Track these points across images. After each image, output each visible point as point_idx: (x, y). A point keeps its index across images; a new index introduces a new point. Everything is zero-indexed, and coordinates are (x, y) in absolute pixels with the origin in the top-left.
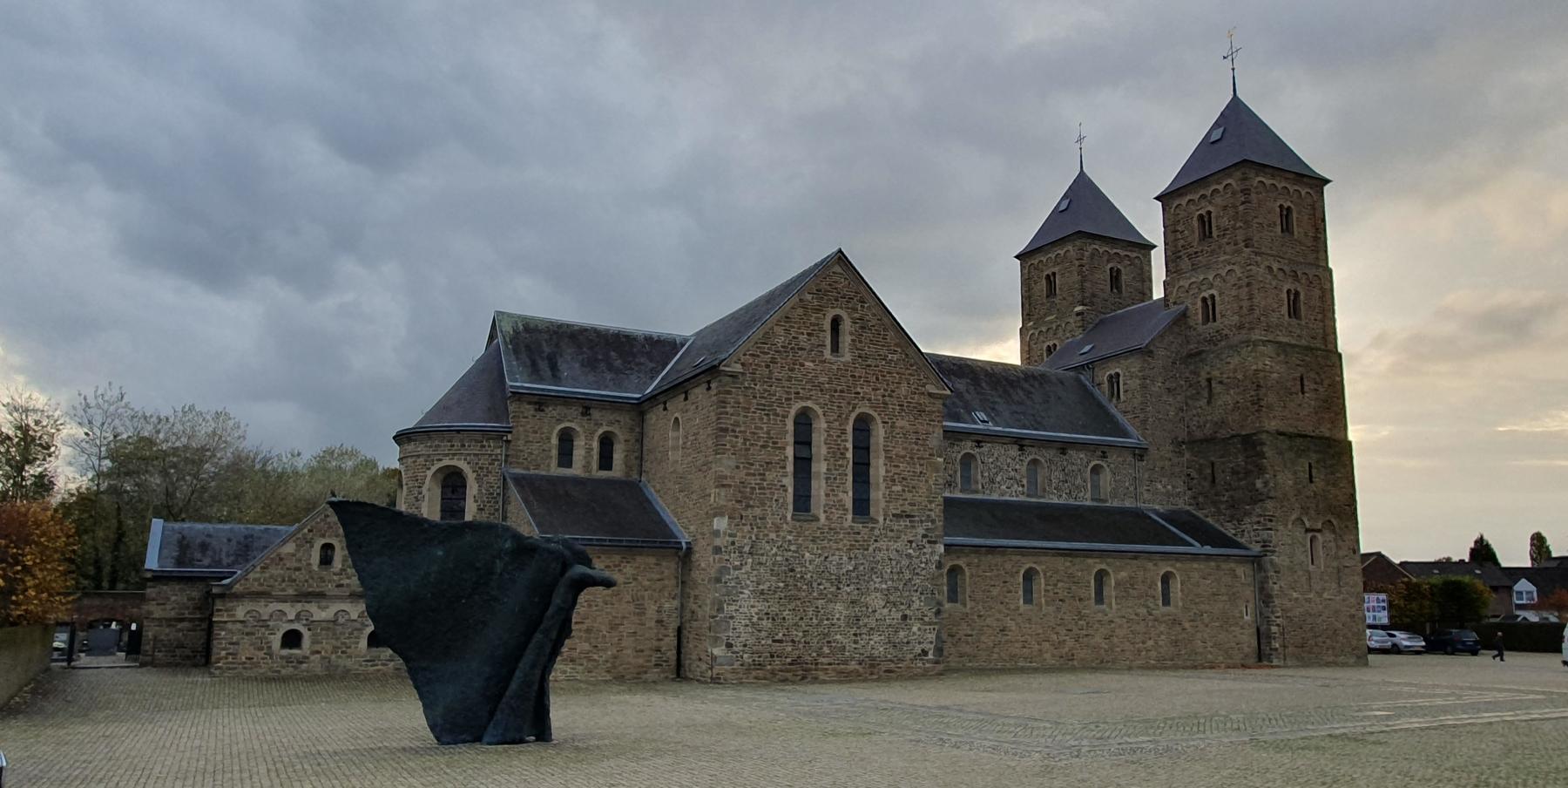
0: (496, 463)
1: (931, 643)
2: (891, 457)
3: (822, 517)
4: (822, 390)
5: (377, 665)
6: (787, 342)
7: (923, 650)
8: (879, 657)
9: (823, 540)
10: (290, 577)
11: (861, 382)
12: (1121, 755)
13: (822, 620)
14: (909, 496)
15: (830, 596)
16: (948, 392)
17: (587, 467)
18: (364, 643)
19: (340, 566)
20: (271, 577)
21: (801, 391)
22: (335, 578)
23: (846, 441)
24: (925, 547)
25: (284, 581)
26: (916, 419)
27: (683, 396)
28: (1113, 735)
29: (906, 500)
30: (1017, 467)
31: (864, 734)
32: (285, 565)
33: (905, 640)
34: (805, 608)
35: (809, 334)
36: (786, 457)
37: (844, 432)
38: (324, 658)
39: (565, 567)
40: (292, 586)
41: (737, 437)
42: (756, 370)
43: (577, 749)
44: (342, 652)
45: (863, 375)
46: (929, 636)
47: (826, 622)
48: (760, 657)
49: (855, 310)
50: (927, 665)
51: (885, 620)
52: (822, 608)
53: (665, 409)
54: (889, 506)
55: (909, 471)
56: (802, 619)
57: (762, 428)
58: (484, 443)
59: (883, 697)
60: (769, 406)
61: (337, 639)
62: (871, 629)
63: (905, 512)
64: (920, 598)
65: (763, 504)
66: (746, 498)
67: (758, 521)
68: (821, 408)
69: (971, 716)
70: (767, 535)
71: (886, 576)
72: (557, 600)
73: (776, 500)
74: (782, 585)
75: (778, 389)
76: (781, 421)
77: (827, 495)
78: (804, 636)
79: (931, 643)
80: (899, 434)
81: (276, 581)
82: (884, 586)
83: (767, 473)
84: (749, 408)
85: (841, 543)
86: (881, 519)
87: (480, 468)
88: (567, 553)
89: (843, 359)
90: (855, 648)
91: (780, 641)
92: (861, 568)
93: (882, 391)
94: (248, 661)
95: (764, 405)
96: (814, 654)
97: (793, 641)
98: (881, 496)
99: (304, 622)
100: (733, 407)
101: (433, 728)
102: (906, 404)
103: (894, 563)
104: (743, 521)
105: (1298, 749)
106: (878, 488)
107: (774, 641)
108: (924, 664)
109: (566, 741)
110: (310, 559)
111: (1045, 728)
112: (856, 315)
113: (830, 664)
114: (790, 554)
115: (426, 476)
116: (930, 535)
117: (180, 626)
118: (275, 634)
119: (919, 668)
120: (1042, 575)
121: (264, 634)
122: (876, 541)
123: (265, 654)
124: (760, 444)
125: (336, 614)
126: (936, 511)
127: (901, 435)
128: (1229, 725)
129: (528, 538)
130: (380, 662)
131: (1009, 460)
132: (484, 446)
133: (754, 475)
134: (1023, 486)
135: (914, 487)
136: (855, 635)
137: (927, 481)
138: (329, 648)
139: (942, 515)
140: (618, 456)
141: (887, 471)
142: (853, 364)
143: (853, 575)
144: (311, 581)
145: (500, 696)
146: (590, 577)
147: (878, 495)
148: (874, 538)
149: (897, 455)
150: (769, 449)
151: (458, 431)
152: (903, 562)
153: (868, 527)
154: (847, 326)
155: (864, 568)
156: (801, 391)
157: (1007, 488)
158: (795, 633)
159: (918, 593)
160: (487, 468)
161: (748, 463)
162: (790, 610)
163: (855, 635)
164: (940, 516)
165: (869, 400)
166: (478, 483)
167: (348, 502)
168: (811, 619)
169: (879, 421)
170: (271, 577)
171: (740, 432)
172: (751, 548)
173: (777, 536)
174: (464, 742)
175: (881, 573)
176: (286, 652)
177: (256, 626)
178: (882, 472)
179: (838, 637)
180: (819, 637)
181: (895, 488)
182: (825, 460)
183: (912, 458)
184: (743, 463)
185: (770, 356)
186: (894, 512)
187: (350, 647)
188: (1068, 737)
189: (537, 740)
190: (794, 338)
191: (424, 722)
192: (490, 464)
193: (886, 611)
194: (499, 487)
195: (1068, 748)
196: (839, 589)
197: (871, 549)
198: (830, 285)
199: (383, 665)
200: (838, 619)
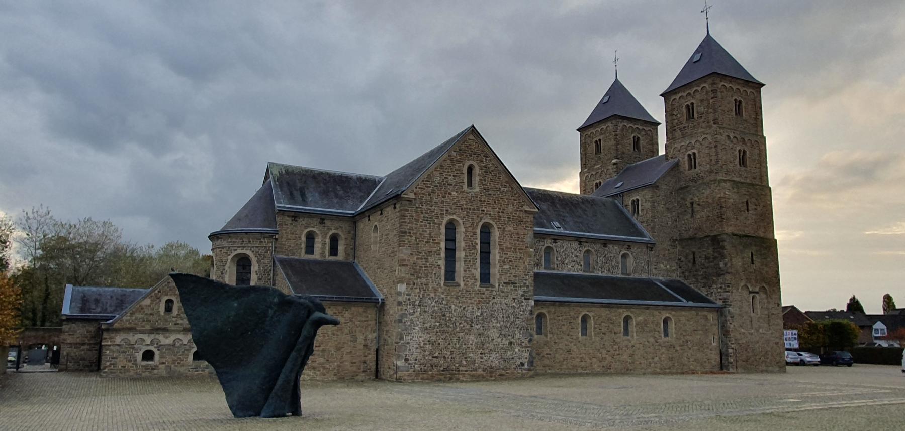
1: (526, 358)
2: (503, 249)
3: (462, 284)
4: (462, 209)
6: (441, 180)
7: (521, 363)
9: (462, 298)
11: (485, 204)
12: (639, 425)
13: (462, 345)
14: (513, 271)
15: (466, 331)
16: (537, 210)
17: (323, 254)
18: (191, 358)
19: (177, 313)
20: (136, 319)
21: (449, 209)
22: (174, 319)
23: (477, 239)
24: (522, 302)
25: (144, 321)
26: (517, 226)
27: (380, 212)
28: (634, 413)
29: (512, 274)
30: (578, 254)
31: (486, 412)
33: (511, 357)
34: (452, 338)
35: (454, 176)
36: (441, 249)
37: (475, 234)
39: (310, 312)
40: (148, 324)
41: (411, 236)
42: (423, 197)
43: (317, 420)
45: (486, 200)
46: (526, 354)
47: (464, 346)
48: (425, 367)
49: (482, 161)
50: (524, 372)
51: (499, 345)
52: (462, 338)
53: (369, 220)
54: (501, 278)
55: (513, 257)
57: (426, 231)
59: (498, 391)
60: (430, 218)
61: (175, 355)
62: (491, 350)
63: (511, 281)
64: (519, 332)
65: (427, 276)
66: (417, 273)
67: (424, 286)
68: (461, 219)
69: (550, 402)
70: (429, 295)
71: (499, 319)
72: (304, 332)
74: (438, 324)
75: (436, 208)
76: (437, 227)
77: (465, 271)
78: (451, 354)
79: (526, 358)
80: (507, 235)
82: (498, 325)
83: (429, 258)
84: (419, 220)
85: (473, 299)
86: (497, 285)
88: (311, 305)
89: (474, 191)
90: (481, 362)
91: (437, 357)
92: (485, 314)
93: (498, 209)
94: (123, 369)
95: (428, 218)
96: (457, 365)
97: (444, 357)
98: (497, 272)
99: (156, 345)
100: (409, 219)
101: (231, 408)
102: (512, 217)
103: (504, 311)
104: (415, 287)
105: (744, 421)
106: (495, 267)
107: (433, 357)
108: (522, 371)
109: (310, 415)
110: (159, 309)
111: (594, 409)
112: (482, 164)
113: (466, 371)
114: (443, 305)
115: (227, 259)
116: (525, 294)
117: (82, 347)
118: (138, 352)
119: (519, 373)
120: (592, 318)
122: (494, 298)
124: (425, 240)
125: (174, 341)
126: (530, 281)
127: (509, 236)
128: (703, 407)
129: (288, 296)
130: (200, 369)
131: (573, 251)
132: (262, 242)
133: (422, 259)
134: (581, 266)
135: (516, 267)
136: (481, 354)
137: (524, 263)
139: (533, 283)
140: (341, 248)
141: (500, 257)
142: (481, 193)
143: (480, 318)
144: (159, 321)
145: (271, 389)
146: (324, 318)
147: (495, 271)
148: (492, 296)
149: (506, 248)
150: (431, 243)
151: (247, 233)
152: (510, 311)
153: (489, 290)
154: (477, 170)
155: (487, 314)
156: (449, 209)
157: (572, 267)
158: (446, 352)
159: (519, 329)
160: (264, 255)
161: (418, 252)
162: (442, 339)
163: (481, 354)
164: (532, 284)
165: (490, 215)
167: (181, 274)
168: (455, 344)
169: (495, 227)
170: (136, 319)
171: (414, 233)
172: (420, 302)
173: (436, 295)
174: (250, 416)
175: (497, 317)
176: (145, 363)
178: (497, 257)
179: (471, 355)
181: (505, 267)
182: (464, 250)
183: (515, 249)
184: (415, 252)
185: (431, 188)
186: (505, 281)
187: (182, 361)
188: (607, 414)
189: (293, 415)
190: (445, 178)
191: (226, 405)
192: (265, 252)
193: (499, 340)
194: (271, 266)
195: (608, 421)
197: (490, 303)
198: (467, 146)
199: (202, 371)
200: (471, 344)
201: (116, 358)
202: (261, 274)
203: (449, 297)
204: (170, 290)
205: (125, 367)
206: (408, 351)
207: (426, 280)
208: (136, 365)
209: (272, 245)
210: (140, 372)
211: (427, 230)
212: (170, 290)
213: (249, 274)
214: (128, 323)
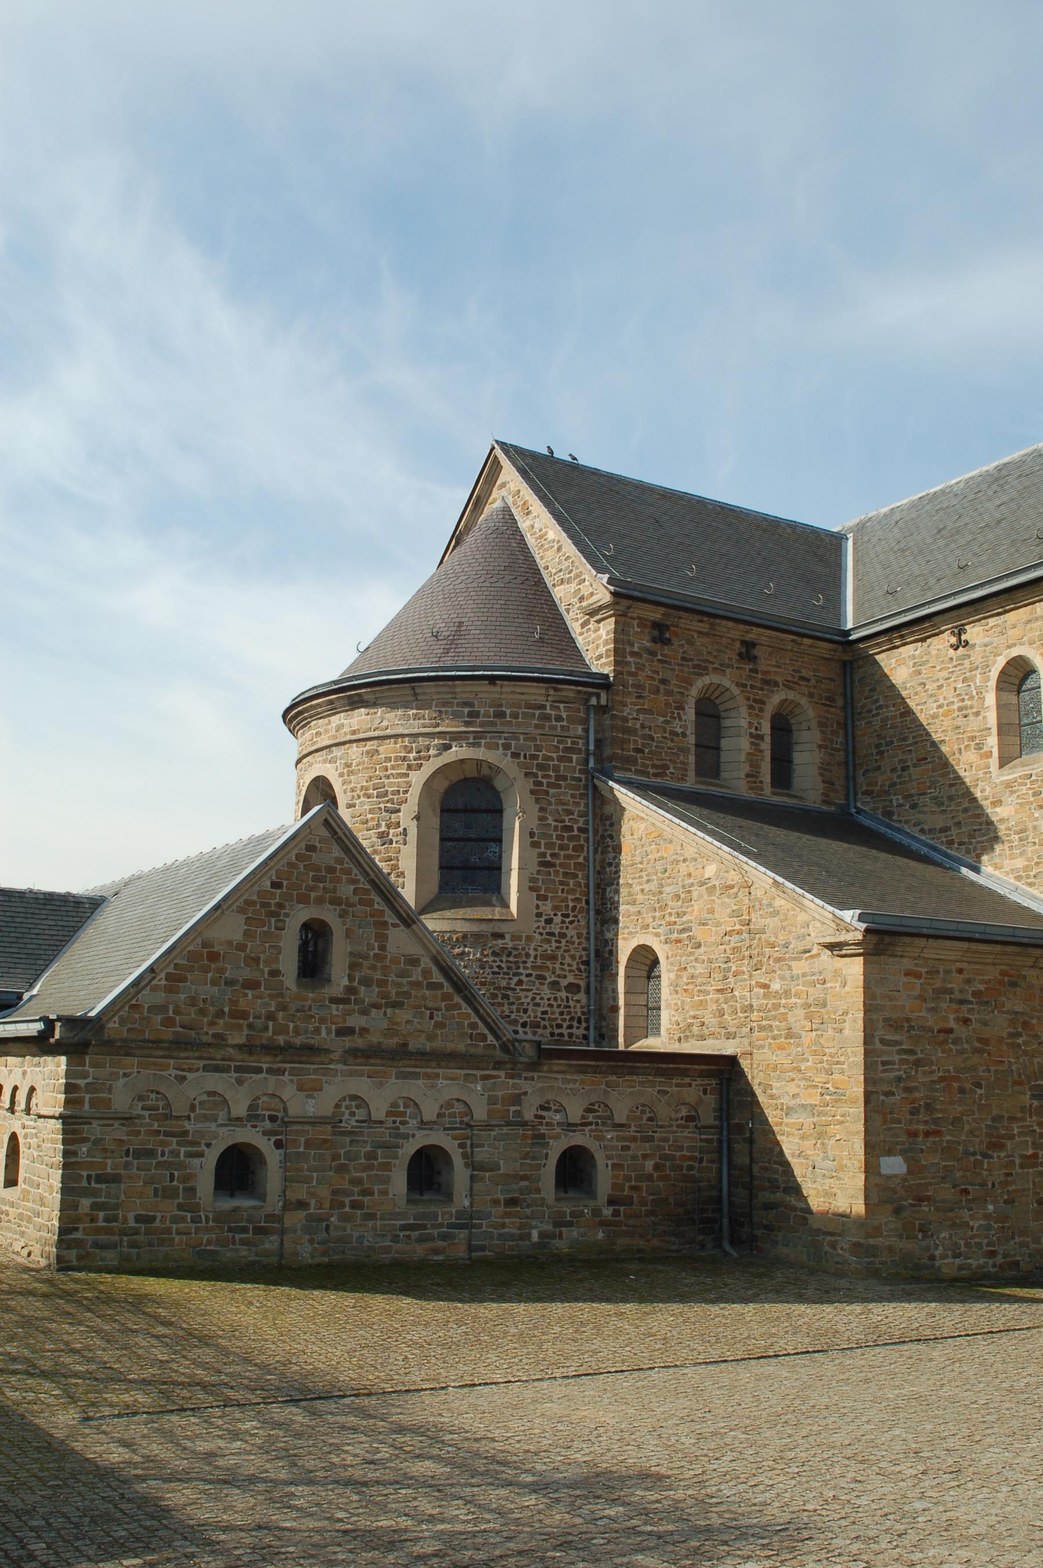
0: (574, 757)
5: (430, 1238)
10: (234, 1002)
17: (753, 776)
18: (399, 1182)
19: (345, 982)
20: (193, 1001)
22: (335, 1010)
25: (220, 1014)
32: (222, 970)
38: (310, 1218)
40: (239, 1027)
44: (354, 1205)
58: (548, 711)
61: (342, 1169)
81: (202, 1012)
87: (540, 767)
99: (267, 1125)
110: (277, 960)
118: (201, 1155)
121: (178, 1155)
123: (180, 1207)
125: (337, 1106)
130: (436, 1232)
132: (546, 718)
138: (324, 1192)
151: (492, 680)
160: (556, 769)
166: (537, 801)
170: (193, 1001)
176: (227, 1204)
177: (159, 1132)
187: (371, 1193)
192: (560, 759)
194: (585, 814)
199: (444, 1237)
201: (115, 1179)
202: (550, 845)
204: (317, 879)
205: (153, 1219)
208: (194, 1208)
209: (587, 731)
210: (209, 1242)
212: (317, 879)
213: (494, 847)
214: (159, 1018)
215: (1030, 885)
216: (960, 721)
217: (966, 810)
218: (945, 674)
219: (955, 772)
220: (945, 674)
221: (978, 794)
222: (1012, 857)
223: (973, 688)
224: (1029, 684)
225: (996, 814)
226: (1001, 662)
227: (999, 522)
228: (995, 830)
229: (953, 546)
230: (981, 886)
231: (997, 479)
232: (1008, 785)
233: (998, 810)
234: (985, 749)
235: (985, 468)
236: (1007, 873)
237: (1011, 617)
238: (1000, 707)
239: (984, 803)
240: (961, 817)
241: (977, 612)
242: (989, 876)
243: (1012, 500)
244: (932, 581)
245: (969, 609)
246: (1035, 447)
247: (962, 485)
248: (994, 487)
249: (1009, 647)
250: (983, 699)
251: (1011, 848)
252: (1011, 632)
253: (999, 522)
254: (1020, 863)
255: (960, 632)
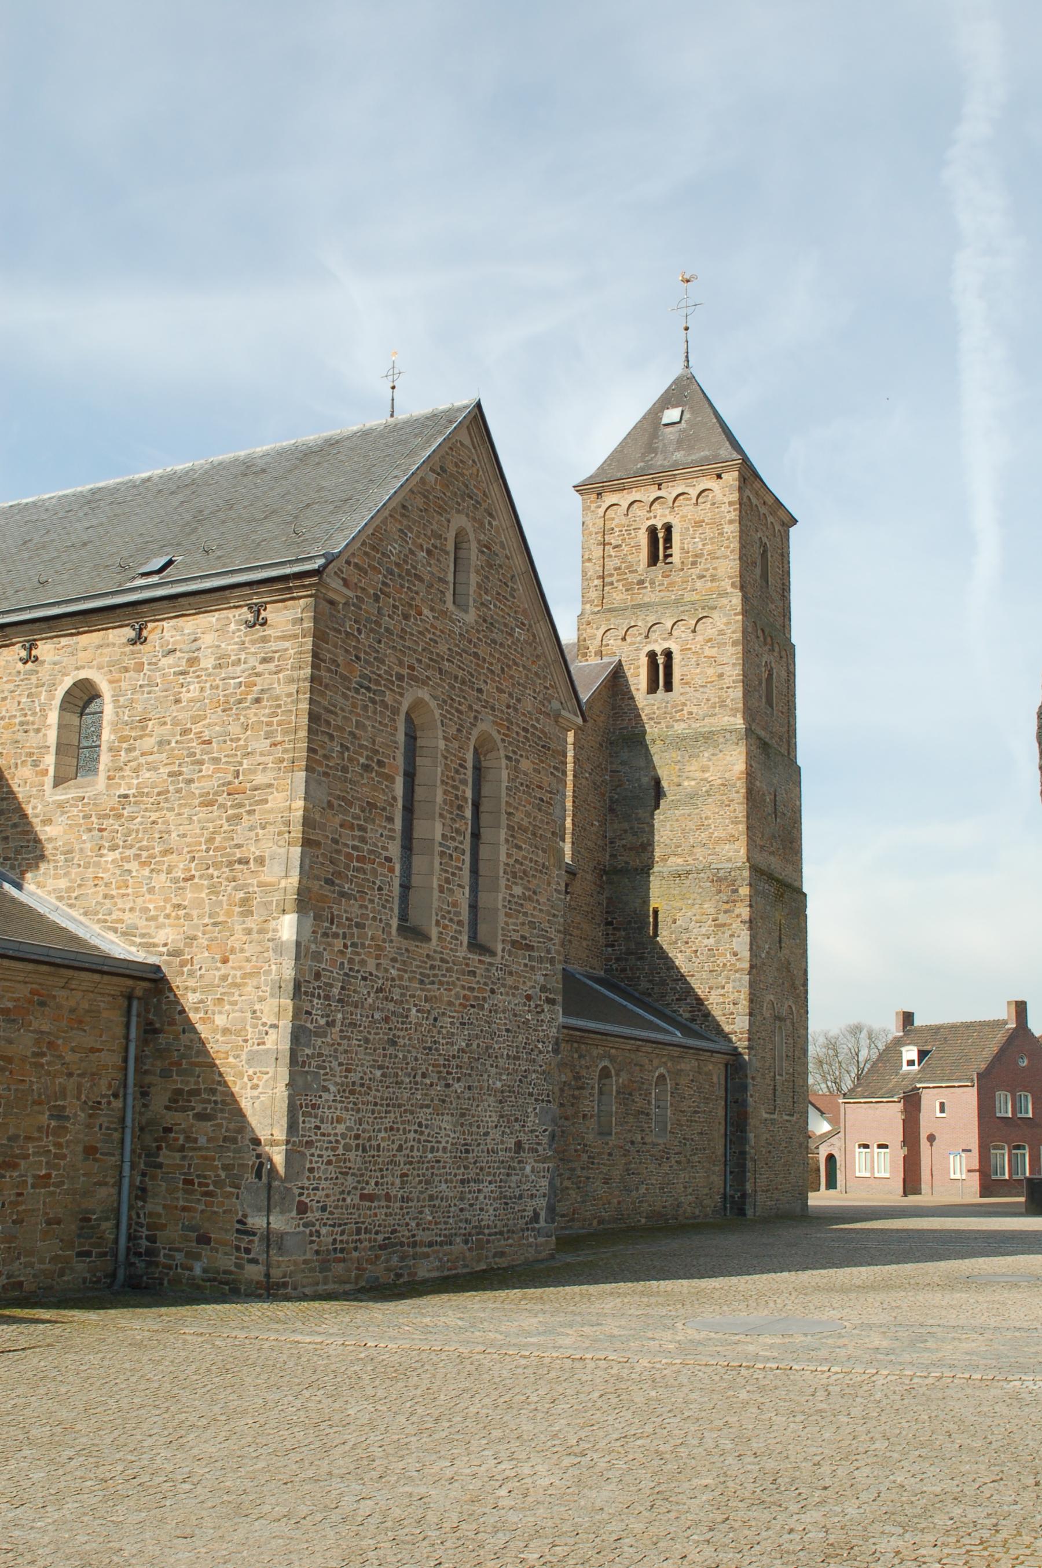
8: (488, 1227)
27: (129, 633)
36: (394, 798)
56: (400, 1148)
70: (363, 962)
73: (380, 889)
74: (378, 1073)
83: (369, 827)
97: (388, 1197)
106: (495, 889)
107: (363, 1197)
150: (374, 774)
172: (343, 988)
180: (419, 1188)
196: (448, 1086)
203: (406, 976)
206: (307, 1174)
207: (361, 907)
211: (367, 723)
215: (71, 906)
216: (20, 736)
217: (15, 826)
218: (11, 686)
219: (9, 786)
220: (11, 686)
221: (29, 811)
222: (56, 877)
223: (37, 704)
224: (93, 707)
225: (45, 832)
226: (68, 682)
227: (85, 544)
228: (42, 849)
229: (36, 560)
230: (21, 903)
231: (89, 502)
232: (61, 805)
233: (47, 828)
234: (42, 767)
235: (79, 489)
236: (49, 893)
237: (84, 639)
238: (61, 726)
239: (35, 821)
240: (9, 832)
241: (51, 629)
242: (31, 894)
243: (102, 524)
244: (10, 592)
245: (43, 625)
246: (131, 477)
247: (54, 501)
248: (86, 509)
249: (77, 669)
250: (46, 717)
251: (56, 868)
252: (81, 655)
253: (85, 544)
254: (63, 883)
255: (31, 646)
